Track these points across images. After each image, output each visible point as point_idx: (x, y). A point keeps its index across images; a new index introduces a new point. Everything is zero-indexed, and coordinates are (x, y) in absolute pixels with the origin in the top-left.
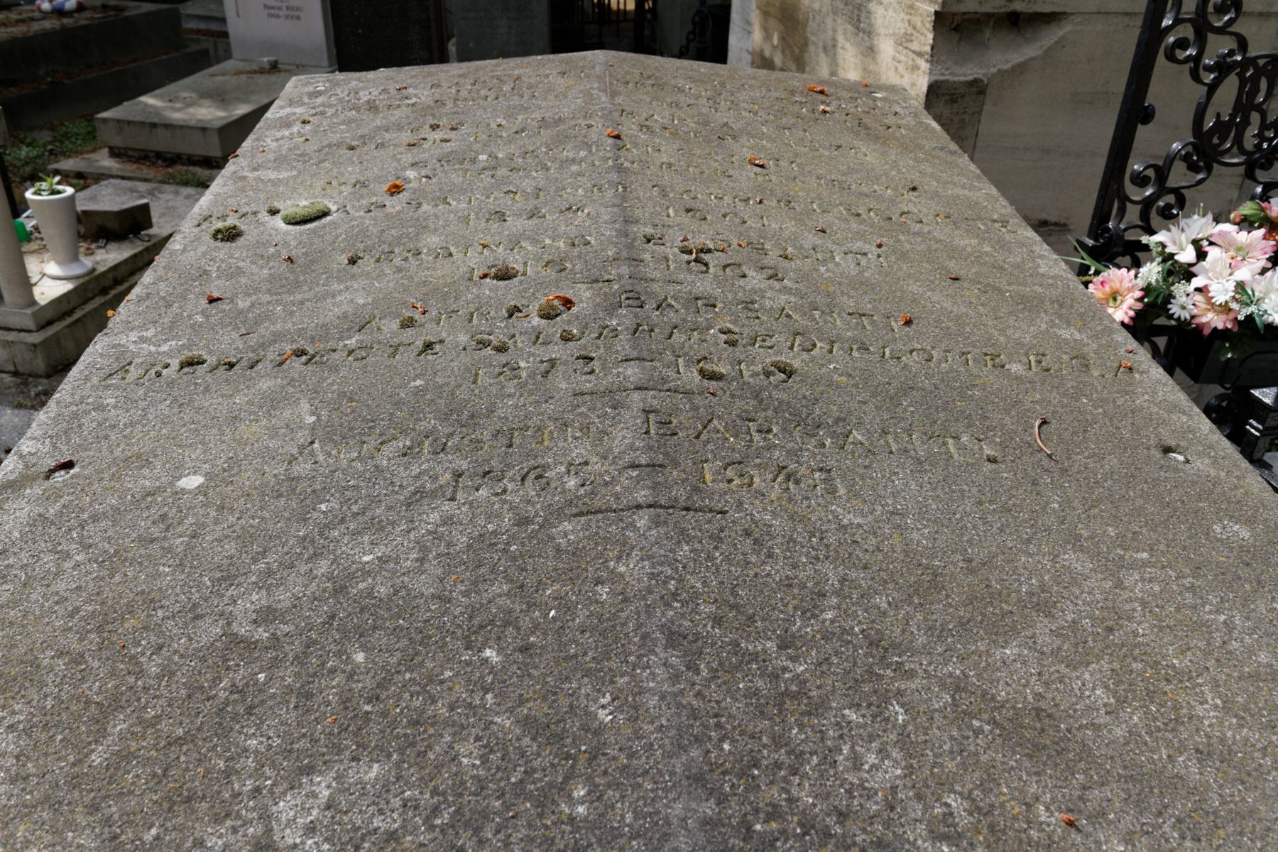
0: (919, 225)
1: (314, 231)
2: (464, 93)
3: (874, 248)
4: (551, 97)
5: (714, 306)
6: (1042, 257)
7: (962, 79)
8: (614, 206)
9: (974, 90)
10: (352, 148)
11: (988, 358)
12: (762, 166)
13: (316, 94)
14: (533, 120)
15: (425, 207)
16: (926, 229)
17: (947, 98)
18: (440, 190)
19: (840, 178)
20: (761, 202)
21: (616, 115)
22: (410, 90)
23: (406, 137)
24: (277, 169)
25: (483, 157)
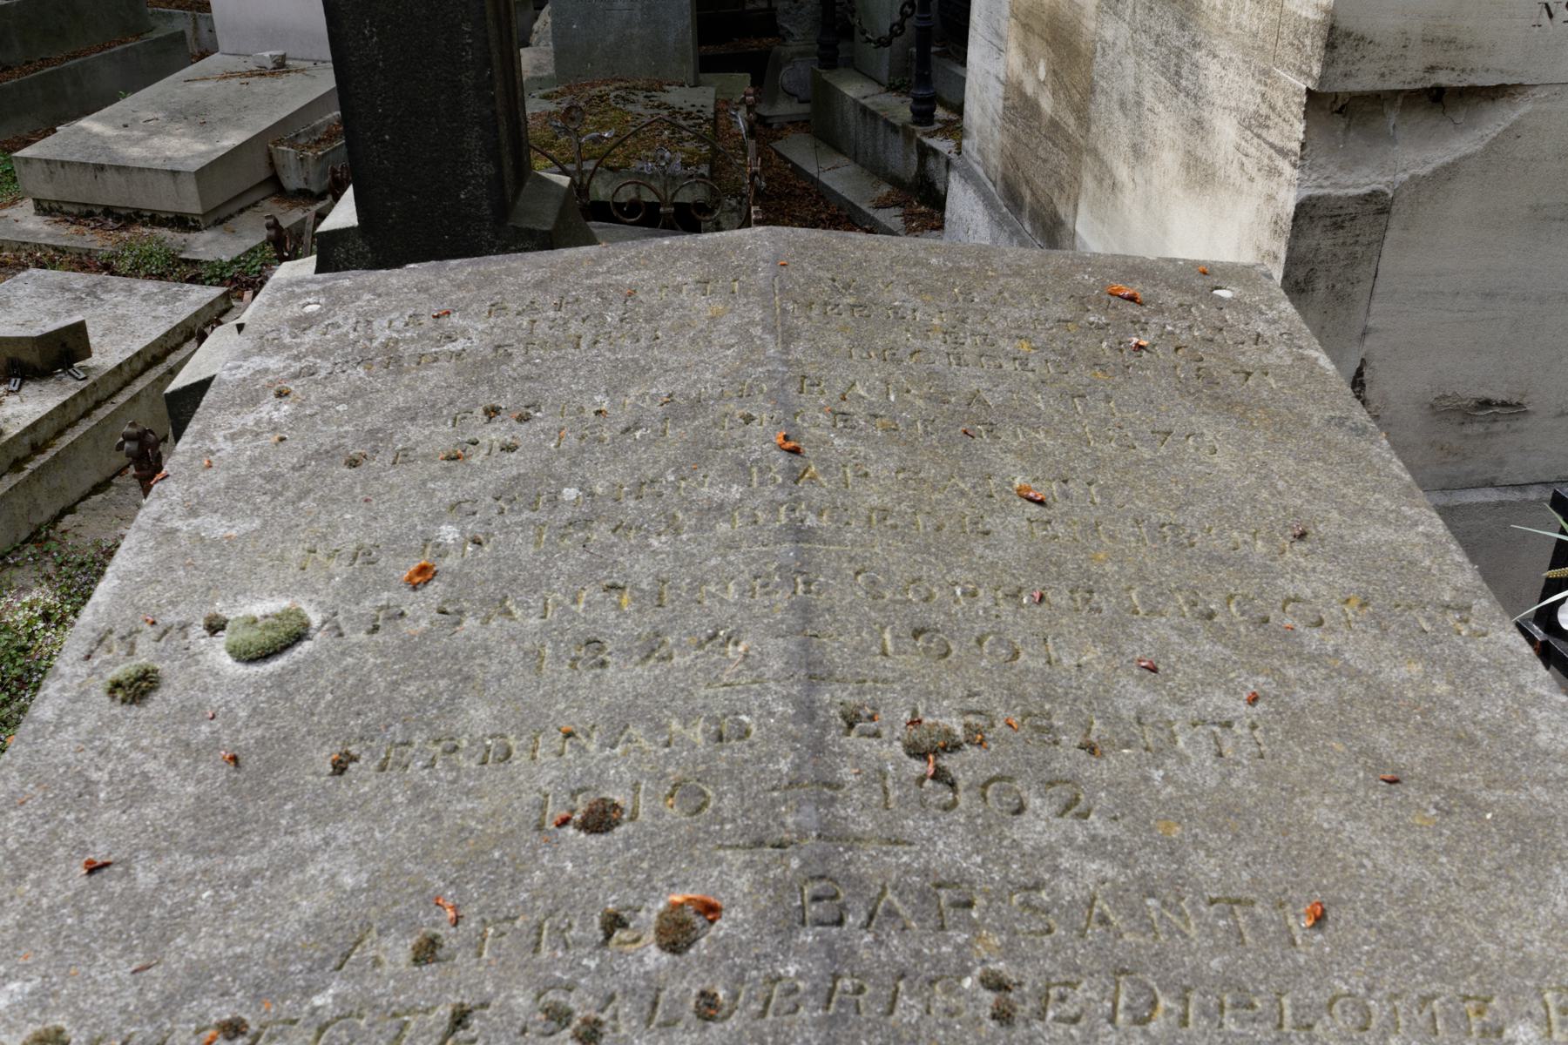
0: (1317, 633)
1: (280, 680)
2: (542, 328)
3: (1244, 707)
4: (684, 343)
5: (969, 904)
6: (1538, 700)
7: (1352, 192)
8: (790, 632)
9: (1371, 207)
10: (353, 463)
11: (1471, 1006)
12: (1041, 503)
13: (303, 323)
14: (654, 398)
15: (470, 623)
16: (1331, 642)
17: (1328, 222)
18: (498, 576)
19: (1175, 518)
20: (1042, 598)
21: (792, 389)
22: (455, 319)
23: (443, 436)
24: (228, 513)
25: (570, 493)
